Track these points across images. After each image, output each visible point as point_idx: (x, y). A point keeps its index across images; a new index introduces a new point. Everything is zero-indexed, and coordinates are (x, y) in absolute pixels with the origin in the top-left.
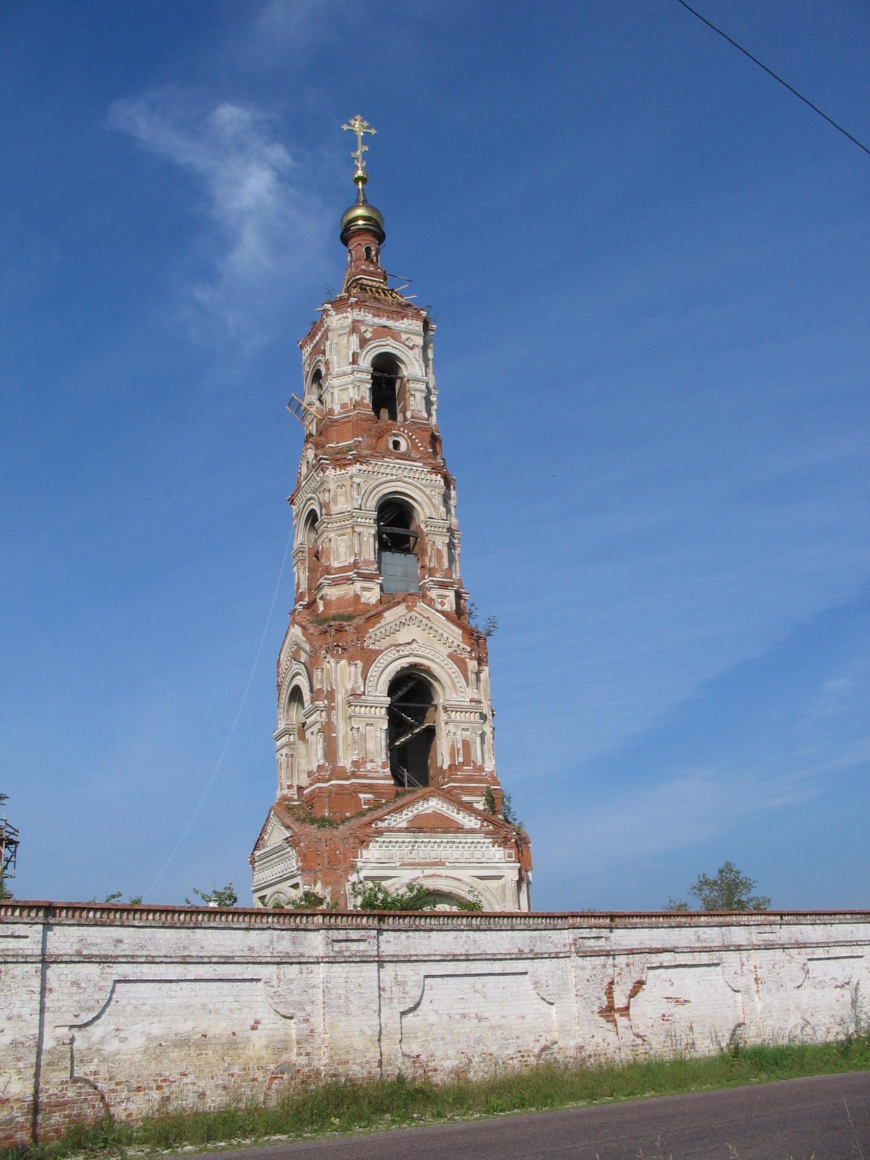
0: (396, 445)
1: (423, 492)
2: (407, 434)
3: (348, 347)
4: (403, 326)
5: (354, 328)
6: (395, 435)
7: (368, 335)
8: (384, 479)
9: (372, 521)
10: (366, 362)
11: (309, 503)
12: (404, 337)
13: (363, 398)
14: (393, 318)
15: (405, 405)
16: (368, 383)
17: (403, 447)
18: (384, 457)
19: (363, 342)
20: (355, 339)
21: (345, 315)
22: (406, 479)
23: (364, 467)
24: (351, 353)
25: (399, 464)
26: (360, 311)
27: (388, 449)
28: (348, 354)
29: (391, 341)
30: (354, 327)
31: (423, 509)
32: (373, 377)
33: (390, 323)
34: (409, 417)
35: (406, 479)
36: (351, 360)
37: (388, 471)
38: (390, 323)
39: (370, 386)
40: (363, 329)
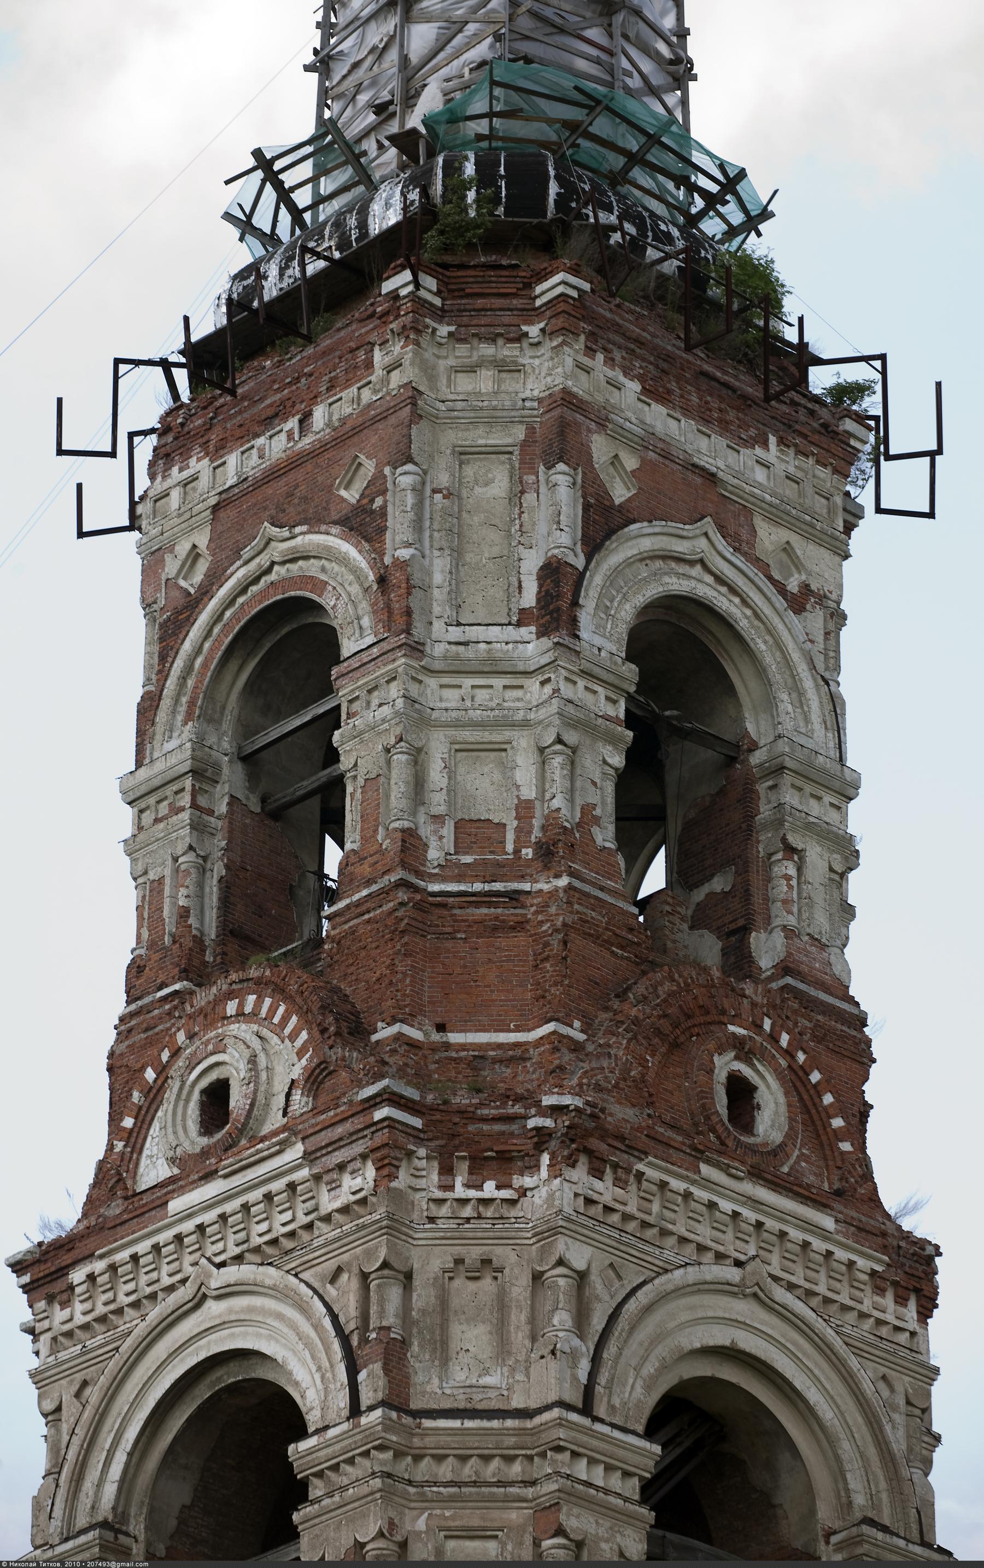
0: (741, 1092)
1: (849, 1379)
2: (789, 1054)
3: (516, 530)
4: (760, 475)
5: (562, 432)
6: (744, 1051)
7: (620, 493)
8: (692, 1274)
9: (632, 1488)
10: (604, 629)
11: (213, 1309)
12: (769, 537)
13: (588, 817)
14: (724, 427)
15: (742, 892)
16: (612, 740)
17: (772, 1115)
18: (699, 1154)
19: (601, 523)
20: (559, 490)
21: (507, 351)
22: (780, 1294)
23: (605, 1189)
24: (532, 562)
25: (755, 1203)
26: (590, 352)
27: (707, 1111)
28: (510, 564)
29: (700, 540)
30: (563, 428)
31: (839, 1474)
32: (631, 721)
33: (709, 449)
34: (766, 962)
35: (780, 1294)
36: (529, 598)
37: (704, 1233)
38: (709, 449)
39: (618, 760)
40: (600, 448)
